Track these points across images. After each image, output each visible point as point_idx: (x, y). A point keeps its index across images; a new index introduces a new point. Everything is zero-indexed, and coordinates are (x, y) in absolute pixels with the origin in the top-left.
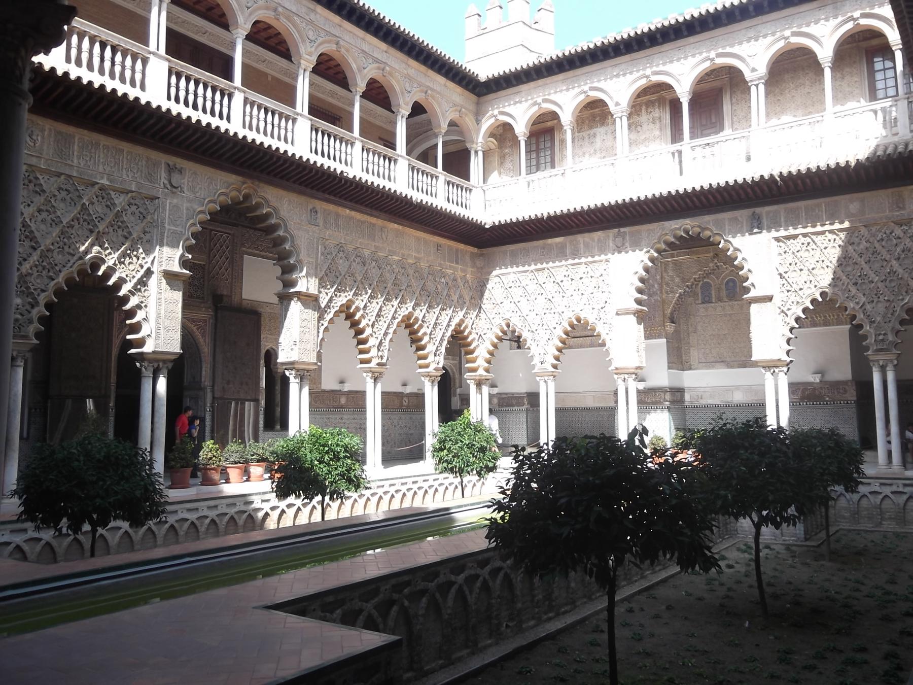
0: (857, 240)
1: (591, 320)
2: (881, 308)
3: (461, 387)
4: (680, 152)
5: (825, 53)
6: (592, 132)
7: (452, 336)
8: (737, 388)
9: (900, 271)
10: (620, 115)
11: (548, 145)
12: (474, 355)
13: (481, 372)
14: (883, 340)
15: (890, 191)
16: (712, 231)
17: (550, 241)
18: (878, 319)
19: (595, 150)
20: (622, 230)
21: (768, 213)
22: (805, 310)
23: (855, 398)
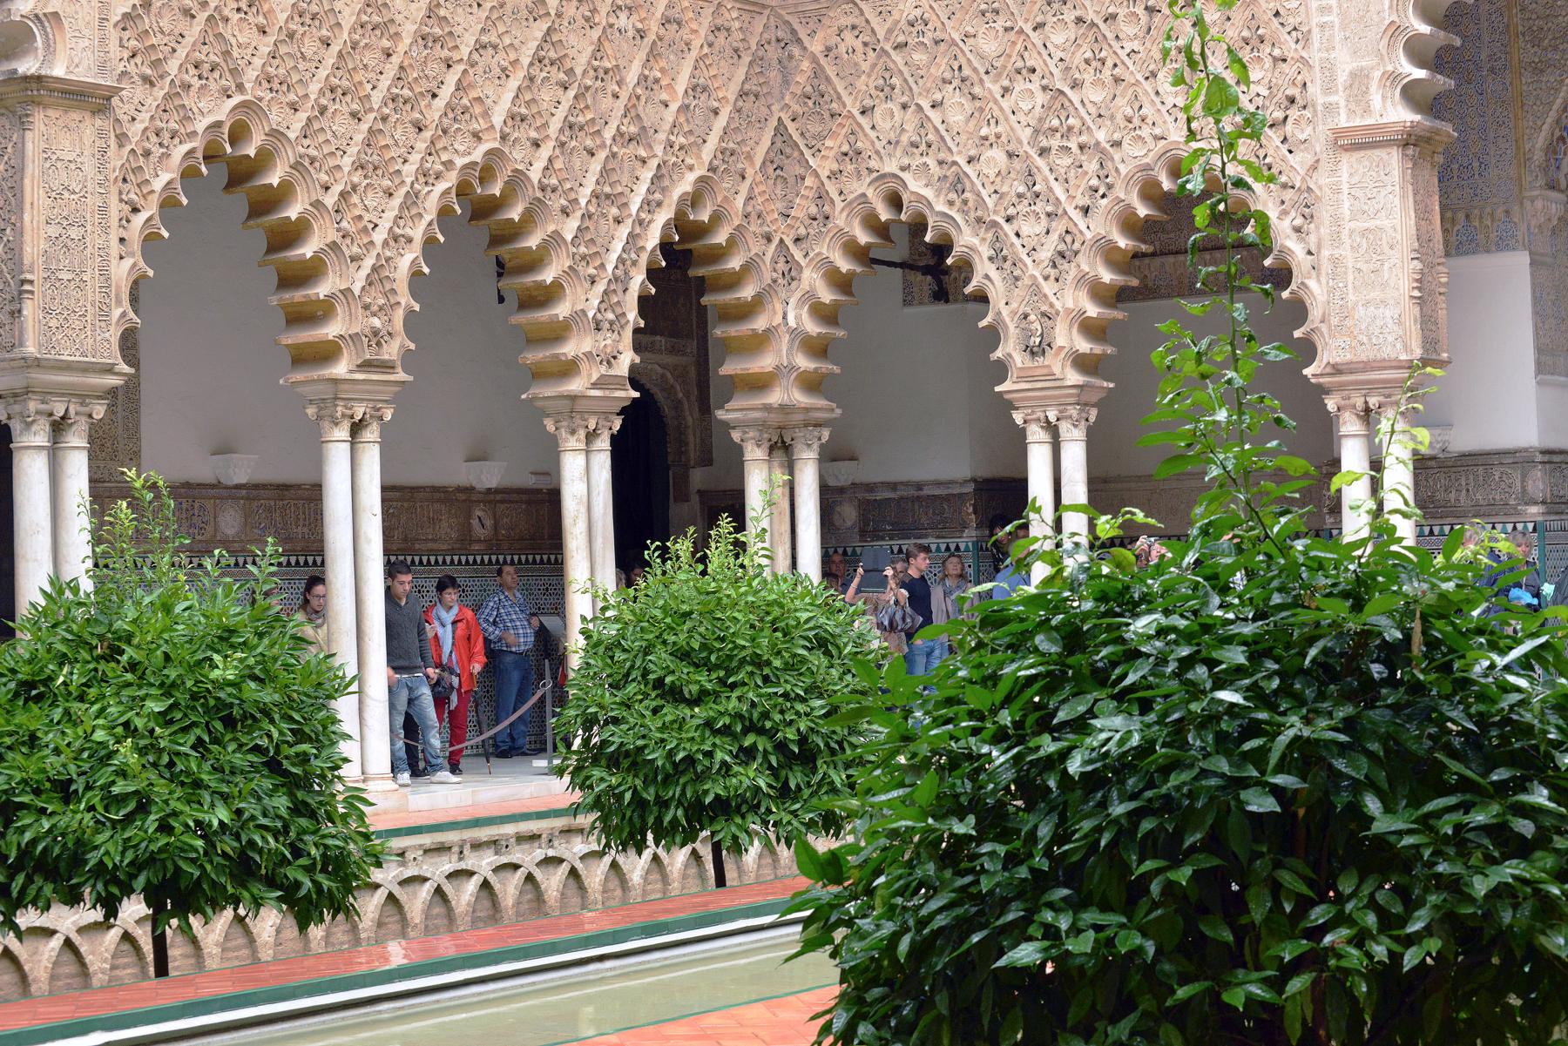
3: (707, 460)
7: (665, 247)
12: (760, 323)
13: (783, 394)
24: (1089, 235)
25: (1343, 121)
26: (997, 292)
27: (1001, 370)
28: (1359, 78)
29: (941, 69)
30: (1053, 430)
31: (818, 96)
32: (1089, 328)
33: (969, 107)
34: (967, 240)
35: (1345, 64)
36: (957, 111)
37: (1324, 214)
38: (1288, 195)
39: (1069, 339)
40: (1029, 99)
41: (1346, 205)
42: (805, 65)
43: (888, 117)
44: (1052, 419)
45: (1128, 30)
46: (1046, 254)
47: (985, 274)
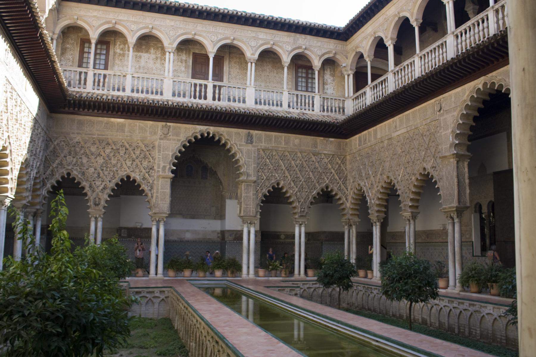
0: (296, 158)
1: (138, 178)
2: (304, 195)
4: (206, 86)
5: (286, 59)
6: (139, 54)
8: (188, 231)
9: (313, 177)
10: (170, 50)
11: (104, 52)
14: (303, 211)
15: (312, 137)
16: (225, 138)
17: (113, 120)
18: (302, 200)
19: (140, 67)
20: (168, 124)
21: (256, 134)
22: (269, 191)
23: (260, 240)
24: (110, 186)
25: (161, 173)
26: (89, 194)
27: (89, 207)
28: (164, 167)
29: (82, 152)
30: (96, 218)
31: (54, 152)
32: (107, 201)
33: (87, 160)
34: (84, 184)
35: (162, 164)
36: (85, 160)
37: (155, 187)
38: (149, 184)
39: (103, 203)
40: (101, 161)
41: (160, 187)
42: (53, 146)
43: (69, 159)
44: (97, 216)
45: (121, 152)
46: (101, 188)
47: (87, 190)
